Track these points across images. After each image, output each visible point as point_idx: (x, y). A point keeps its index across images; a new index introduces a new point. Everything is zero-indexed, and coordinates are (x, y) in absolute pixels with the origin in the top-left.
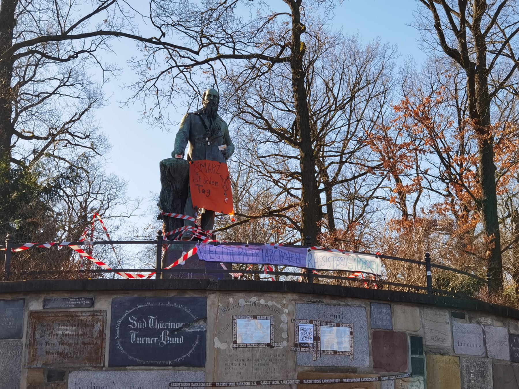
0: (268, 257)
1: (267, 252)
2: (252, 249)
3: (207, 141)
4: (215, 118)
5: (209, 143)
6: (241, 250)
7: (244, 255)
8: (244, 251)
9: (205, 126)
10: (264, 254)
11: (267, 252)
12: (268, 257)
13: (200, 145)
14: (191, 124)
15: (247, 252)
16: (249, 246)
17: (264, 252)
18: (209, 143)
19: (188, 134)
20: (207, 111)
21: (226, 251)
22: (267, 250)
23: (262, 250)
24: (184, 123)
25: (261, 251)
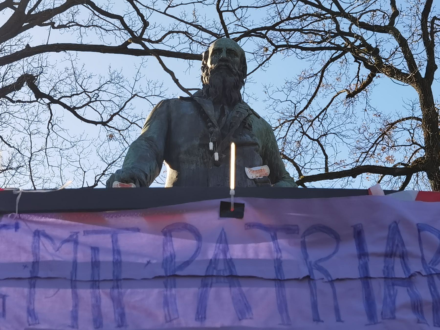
0: (409, 281)
1: (395, 252)
2: (273, 232)
3: (212, 153)
4: (234, 104)
5: (216, 156)
6: (182, 245)
7: (207, 279)
8: (211, 251)
9: (205, 117)
10: (376, 268)
11: (395, 252)
12: (409, 281)
13: (193, 167)
14: (169, 121)
15: (236, 251)
16: (250, 214)
17: (375, 246)
18: (216, 156)
19: (161, 145)
20: (211, 90)
21: (66, 253)
22: (394, 230)
23: (358, 235)
24: (150, 122)
25: (350, 248)
